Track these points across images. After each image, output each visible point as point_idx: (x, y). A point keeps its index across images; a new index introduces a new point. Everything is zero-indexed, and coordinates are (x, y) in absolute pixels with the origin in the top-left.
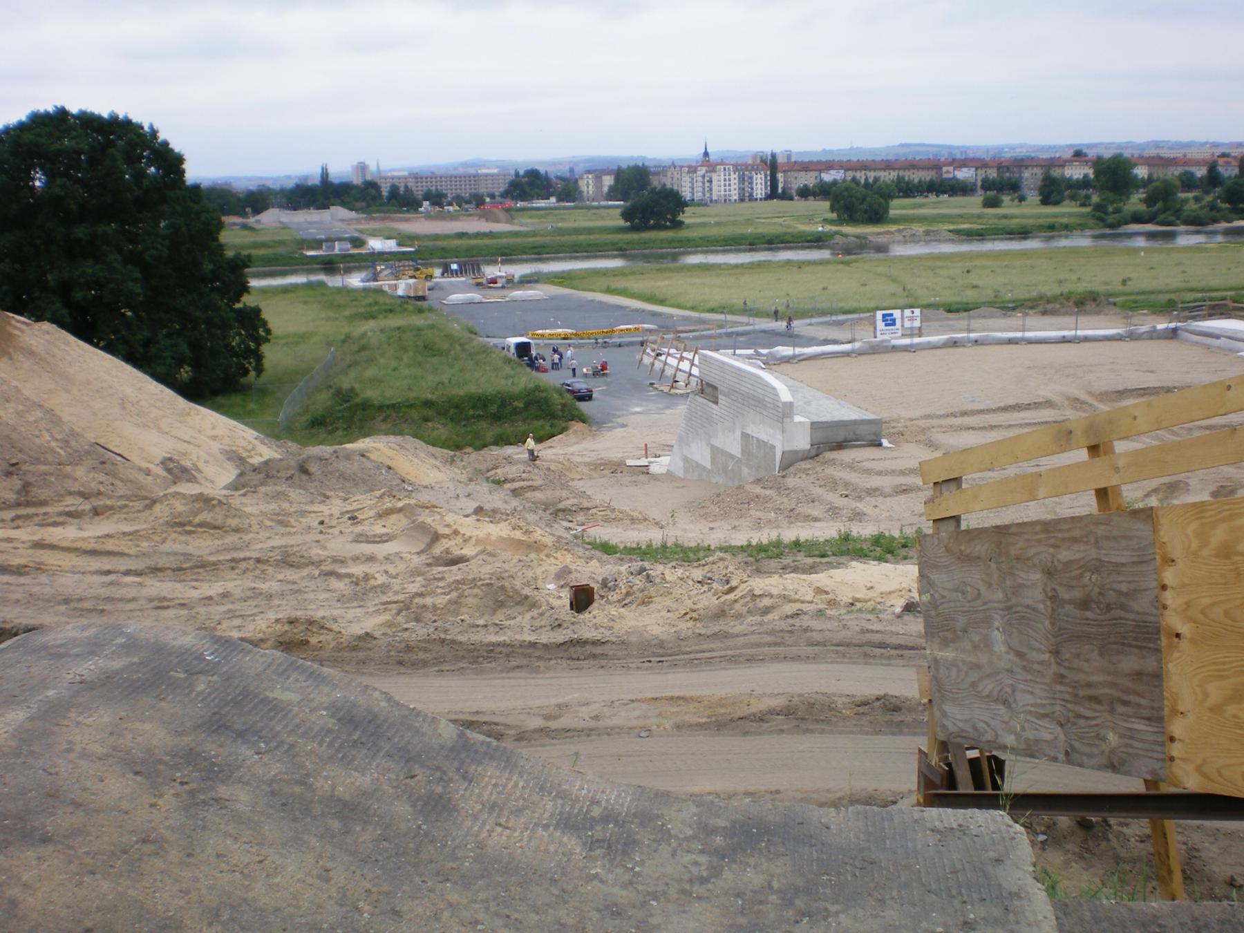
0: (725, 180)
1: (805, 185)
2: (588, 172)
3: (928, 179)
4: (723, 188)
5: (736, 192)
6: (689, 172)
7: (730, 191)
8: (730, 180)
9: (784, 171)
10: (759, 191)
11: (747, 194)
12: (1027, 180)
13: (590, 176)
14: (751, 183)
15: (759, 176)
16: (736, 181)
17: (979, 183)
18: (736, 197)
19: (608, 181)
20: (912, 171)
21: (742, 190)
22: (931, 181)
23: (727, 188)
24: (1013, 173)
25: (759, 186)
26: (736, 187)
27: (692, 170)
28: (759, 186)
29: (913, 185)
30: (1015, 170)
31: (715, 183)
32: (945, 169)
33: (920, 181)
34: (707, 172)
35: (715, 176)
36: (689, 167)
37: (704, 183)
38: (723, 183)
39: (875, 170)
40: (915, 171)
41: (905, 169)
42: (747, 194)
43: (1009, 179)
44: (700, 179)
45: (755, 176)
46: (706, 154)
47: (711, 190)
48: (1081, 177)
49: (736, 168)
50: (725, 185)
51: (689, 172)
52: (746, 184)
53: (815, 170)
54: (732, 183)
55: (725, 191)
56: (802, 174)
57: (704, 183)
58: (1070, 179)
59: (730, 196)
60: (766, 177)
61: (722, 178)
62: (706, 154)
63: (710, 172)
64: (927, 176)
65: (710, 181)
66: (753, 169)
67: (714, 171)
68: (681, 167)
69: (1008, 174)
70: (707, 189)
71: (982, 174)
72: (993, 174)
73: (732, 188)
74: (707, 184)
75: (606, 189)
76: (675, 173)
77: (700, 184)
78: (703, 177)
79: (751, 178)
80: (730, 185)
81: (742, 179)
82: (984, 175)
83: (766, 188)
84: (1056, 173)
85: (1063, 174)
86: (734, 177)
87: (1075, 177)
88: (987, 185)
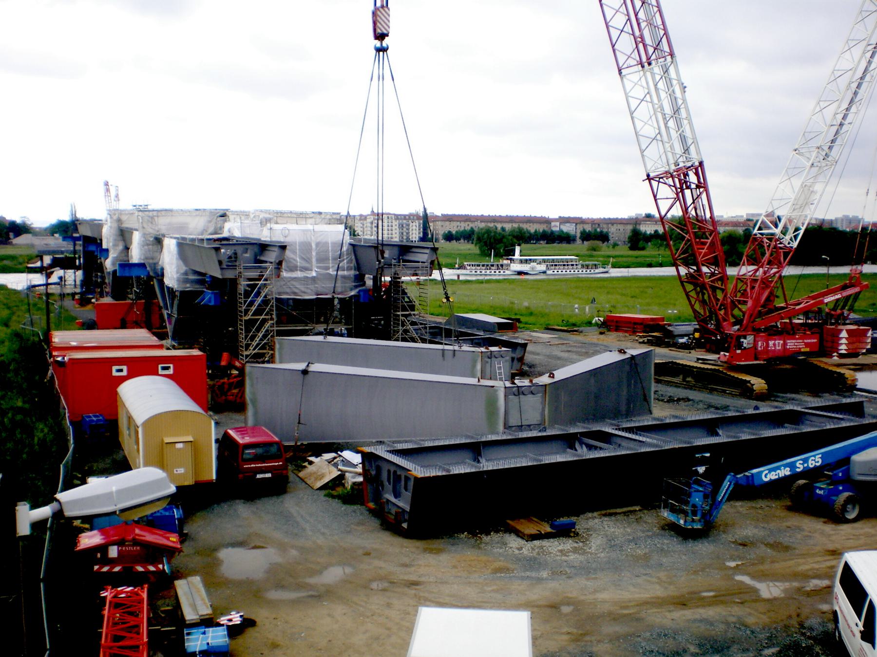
1: (449, 232)
3: (541, 231)
6: (360, 220)
9: (433, 221)
10: (414, 235)
11: (405, 237)
12: (613, 234)
14: (408, 229)
15: (414, 224)
16: (397, 227)
17: (578, 235)
20: (528, 224)
22: (544, 231)
23: (390, 232)
24: (603, 228)
25: (414, 232)
26: (397, 231)
27: (363, 218)
29: (531, 234)
30: (605, 226)
32: (553, 224)
33: (536, 231)
34: (374, 218)
36: (361, 216)
37: (372, 228)
39: (501, 222)
40: (531, 224)
41: (523, 223)
42: (405, 237)
43: (601, 232)
44: (369, 225)
45: (411, 224)
48: (653, 232)
49: (397, 217)
51: (360, 220)
52: (405, 229)
53: (458, 221)
54: (393, 228)
56: (448, 223)
57: (372, 228)
58: (645, 233)
59: (392, 238)
60: (419, 226)
64: (541, 228)
66: (410, 219)
68: (354, 216)
71: (580, 228)
72: (588, 228)
77: (369, 229)
78: (372, 223)
79: (408, 225)
80: (392, 230)
81: (401, 226)
82: (582, 229)
83: (419, 233)
86: (396, 223)
87: (648, 233)
88: (586, 237)
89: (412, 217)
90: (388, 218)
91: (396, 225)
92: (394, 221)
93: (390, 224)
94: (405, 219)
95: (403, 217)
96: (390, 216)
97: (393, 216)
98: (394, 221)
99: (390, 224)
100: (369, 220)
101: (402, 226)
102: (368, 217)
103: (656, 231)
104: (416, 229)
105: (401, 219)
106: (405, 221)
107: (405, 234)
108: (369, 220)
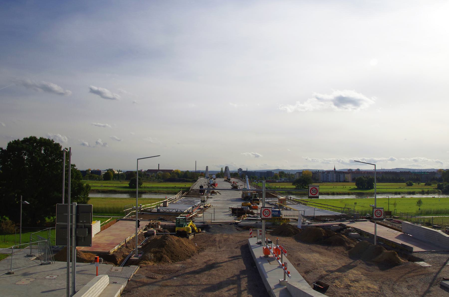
2: (297, 173)
5: (335, 179)
13: (298, 174)
25: (342, 178)
26: (335, 178)
28: (342, 178)
31: (329, 177)
38: (331, 177)
45: (341, 175)
46: (335, 169)
51: (322, 173)
54: (334, 177)
61: (331, 175)
62: (335, 169)
65: (328, 176)
68: (321, 172)
74: (327, 177)
80: (333, 177)
89: (341, 172)
90: (332, 173)
91: (335, 176)
93: (333, 175)
94: (338, 173)
95: (337, 172)
96: (333, 172)
97: (334, 172)
98: (334, 174)
99: (333, 175)
100: (325, 174)
101: (337, 176)
102: (325, 172)
104: (342, 177)
106: (338, 174)
108: (325, 174)
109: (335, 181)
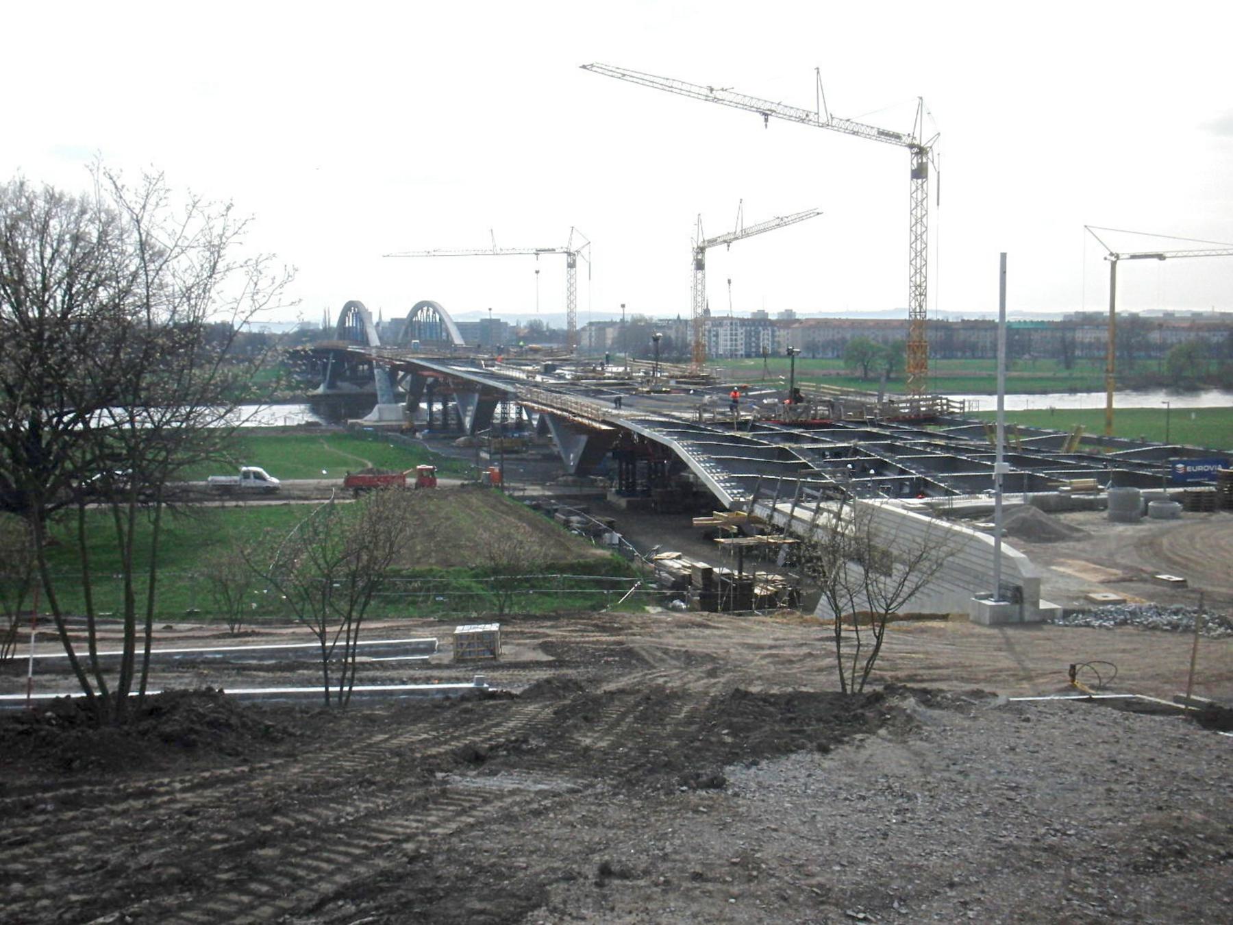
0: (731, 335)
2: (591, 324)
4: (729, 343)
5: (743, 347)
7: (736, 345)
8: (736, 335)
11: (754, 350)
13: (593, 328)
16: (743, 336)
18: (743, 352)
19: (611, 334)
21: (748, 344)
25: (766, 342)
35: (721, 331)
38: (729, 337)
45: (762, 332)
47: (717, 343)
50: (731, 340)
52: (753, 339)
54: (739, 338)
55: (731, 346)
59: (736, 350)
61: (729, 332)
63: (717, 326)
65: (717, 336)
67: (721, 325)
69: (1017, 337)
70: (713, 344)
73: (739, 343)
74: (714, 339)
75: (609, 342)
76: (681, 327)
78: (710, 331)
80: (736, 340)
81: (748, 335)
84: (1069, 335)
85: (1074, 338)
86: (740, 331)
87: (1087, 340)
90: (731, 324)
92: (739, 328)
98: (739, 328)
103: (1098, 339)
105: (749, 325)
107: (753, 344)
109: (743, 352)
